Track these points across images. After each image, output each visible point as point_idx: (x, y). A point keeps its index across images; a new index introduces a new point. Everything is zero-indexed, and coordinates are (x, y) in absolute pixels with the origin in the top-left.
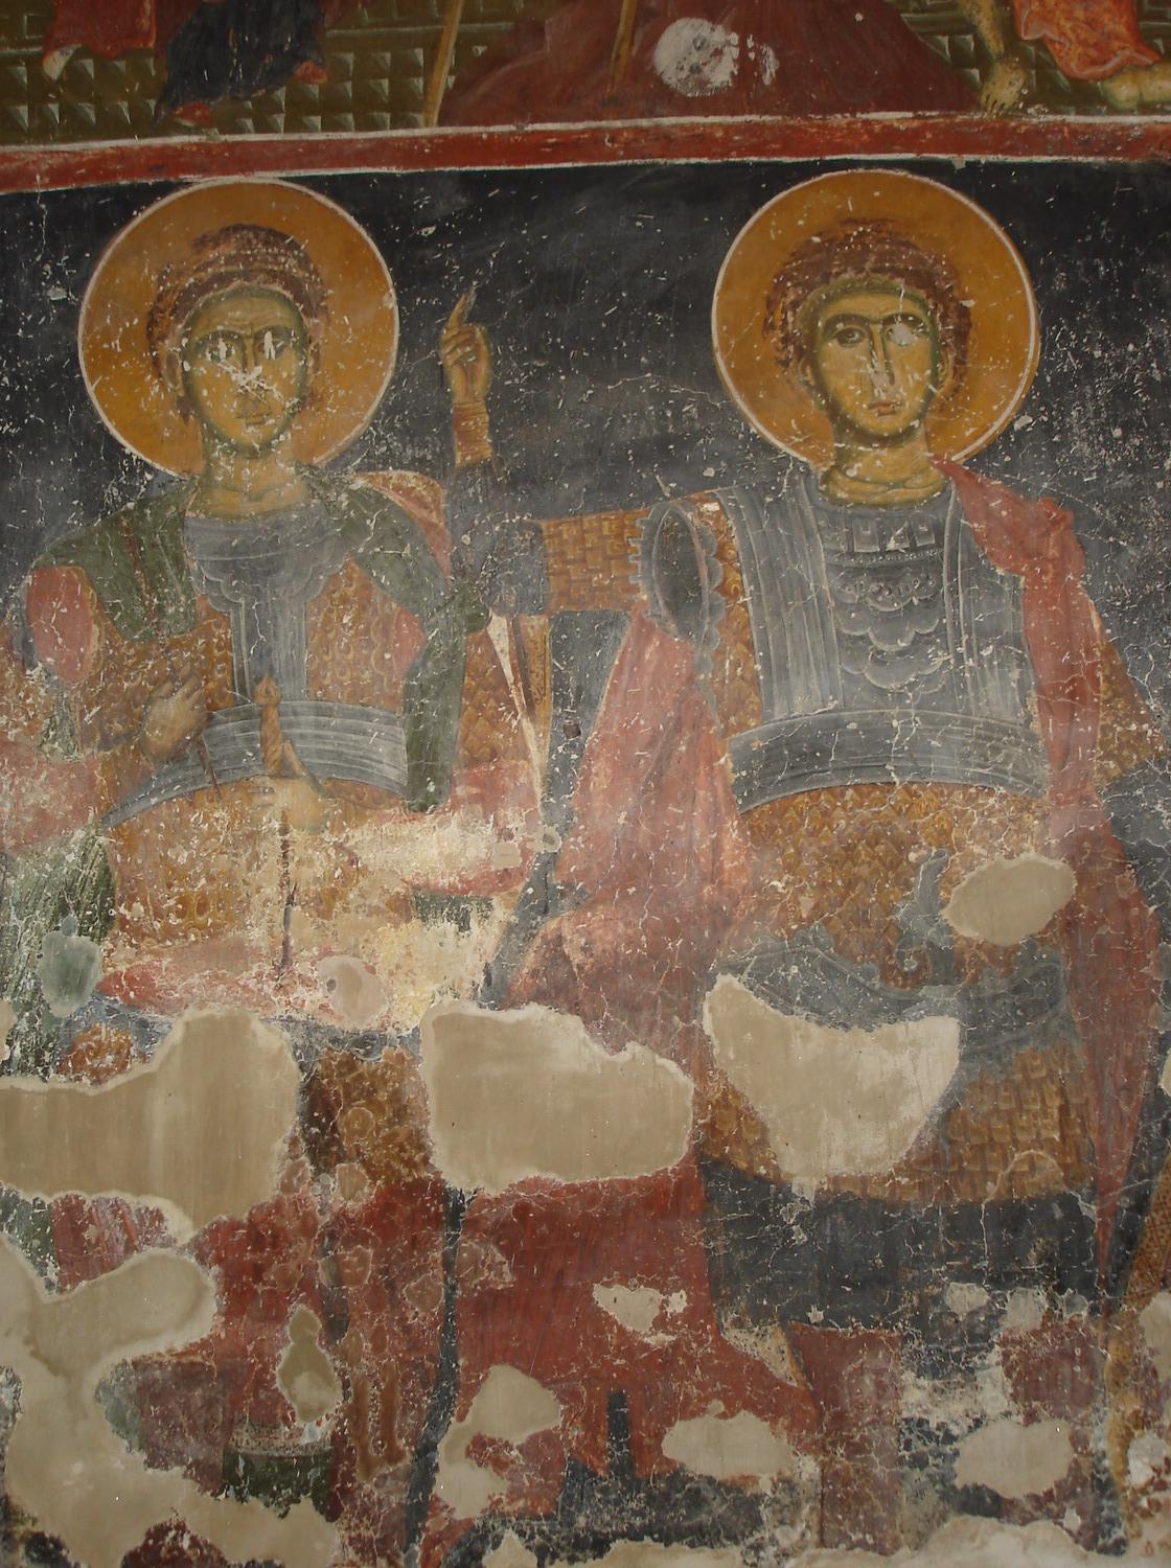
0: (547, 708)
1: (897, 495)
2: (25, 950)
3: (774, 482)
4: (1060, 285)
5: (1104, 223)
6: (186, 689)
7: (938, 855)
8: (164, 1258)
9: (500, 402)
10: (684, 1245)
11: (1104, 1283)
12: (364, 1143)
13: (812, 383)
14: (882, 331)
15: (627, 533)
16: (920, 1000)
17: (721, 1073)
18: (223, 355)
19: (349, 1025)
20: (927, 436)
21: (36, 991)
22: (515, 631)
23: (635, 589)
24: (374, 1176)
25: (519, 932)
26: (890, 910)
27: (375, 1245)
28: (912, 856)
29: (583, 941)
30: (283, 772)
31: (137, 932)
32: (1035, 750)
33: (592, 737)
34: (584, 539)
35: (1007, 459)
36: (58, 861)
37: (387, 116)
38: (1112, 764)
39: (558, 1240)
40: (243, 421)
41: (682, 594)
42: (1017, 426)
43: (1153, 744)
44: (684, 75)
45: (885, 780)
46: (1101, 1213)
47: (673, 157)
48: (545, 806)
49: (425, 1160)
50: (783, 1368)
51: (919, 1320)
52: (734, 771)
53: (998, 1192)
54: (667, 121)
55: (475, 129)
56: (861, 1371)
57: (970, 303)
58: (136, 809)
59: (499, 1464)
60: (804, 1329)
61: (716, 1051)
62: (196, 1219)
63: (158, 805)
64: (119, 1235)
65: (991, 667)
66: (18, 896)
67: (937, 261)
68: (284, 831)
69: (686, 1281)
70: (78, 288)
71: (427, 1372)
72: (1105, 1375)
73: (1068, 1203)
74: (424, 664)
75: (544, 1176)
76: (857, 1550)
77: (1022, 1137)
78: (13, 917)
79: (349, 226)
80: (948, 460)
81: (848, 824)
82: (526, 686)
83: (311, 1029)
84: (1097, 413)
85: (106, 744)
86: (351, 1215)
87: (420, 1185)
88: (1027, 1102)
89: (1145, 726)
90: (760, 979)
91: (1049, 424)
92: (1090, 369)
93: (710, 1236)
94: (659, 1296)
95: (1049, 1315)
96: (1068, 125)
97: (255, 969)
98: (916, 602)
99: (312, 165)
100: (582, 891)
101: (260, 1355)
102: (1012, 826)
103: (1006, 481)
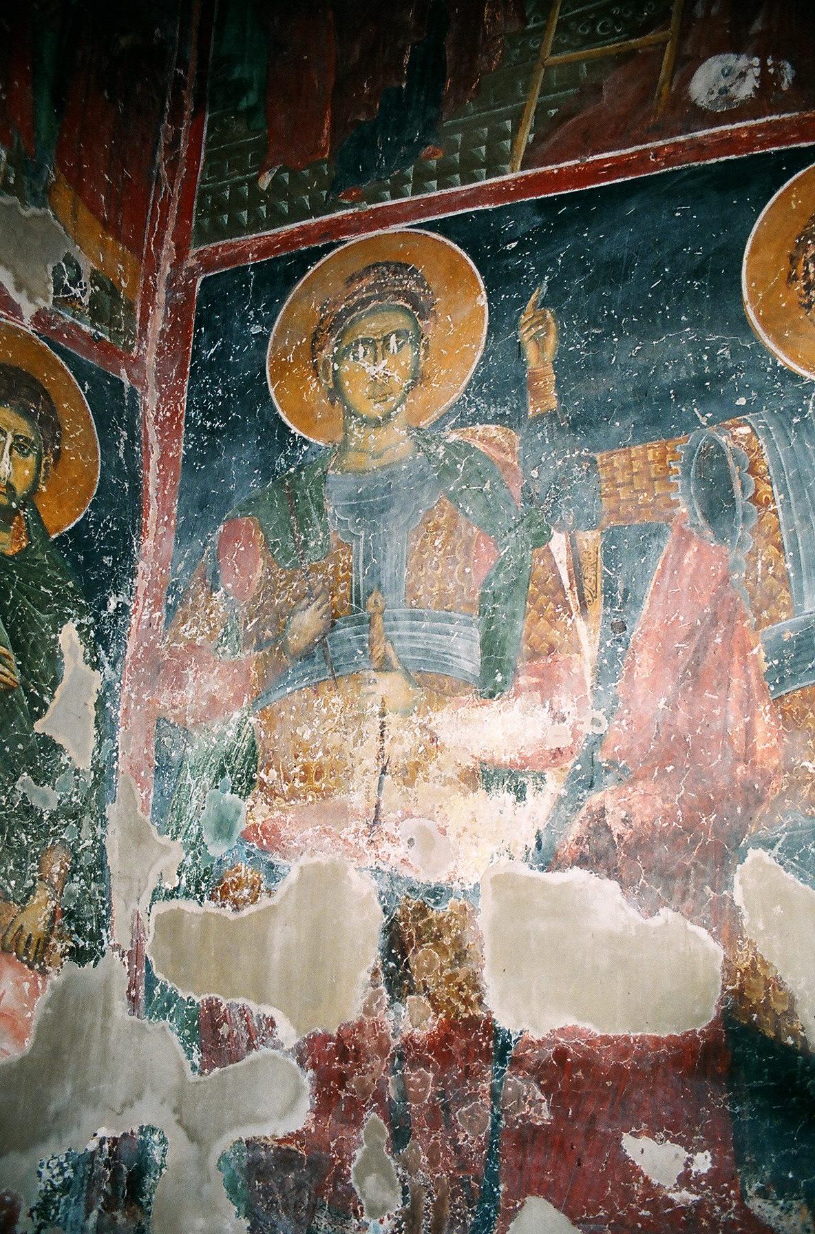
2: (195, 802)
3: (801, 405)
6: (318, 603)
8: (274, 1058)
9: (565, 366)
10: (710, 1107)
12: (430, 980)
15: (669, 457)
17: (750, 943)
18: (361, 355)
19: (424, 877)
21: (199, 835)
22: (572, 544)
24: (437, 1010)
25: (569, 803)
27: (434, 1070)
29: (624, 813)
30: (384, 666)
31: (272, 793)
33: (635, 633)
36: (221, 736)
37: (484, 170)
40: (372, 401)
41: (718, 504)
44: (713, 97)
47: (705, 160)
48: (595, 693)
49: (480, 1000)
52: (766, 660)
54: (700, 134)
55: (549, 168)
58: (275, 696)
61: (745, 922)
62: (298, 1028)
63: (292, 692)
64: (244, 1034)
68: (383, 714)
69: (711, 1143)
70: (269, 324)
71: (473, 1190)
74: (497, 575)
75: (581, 1026)
78: (189, 777)
79: (454, 251)
82: (580, 590)
83: (394, 879)
85: (259, 647)
86: (417, 1042)
87: (473, 1022)
90: (790, 855)
97: (353, 826)
99: (429, 215)
100: (625, 768)
101: (340, 1153)
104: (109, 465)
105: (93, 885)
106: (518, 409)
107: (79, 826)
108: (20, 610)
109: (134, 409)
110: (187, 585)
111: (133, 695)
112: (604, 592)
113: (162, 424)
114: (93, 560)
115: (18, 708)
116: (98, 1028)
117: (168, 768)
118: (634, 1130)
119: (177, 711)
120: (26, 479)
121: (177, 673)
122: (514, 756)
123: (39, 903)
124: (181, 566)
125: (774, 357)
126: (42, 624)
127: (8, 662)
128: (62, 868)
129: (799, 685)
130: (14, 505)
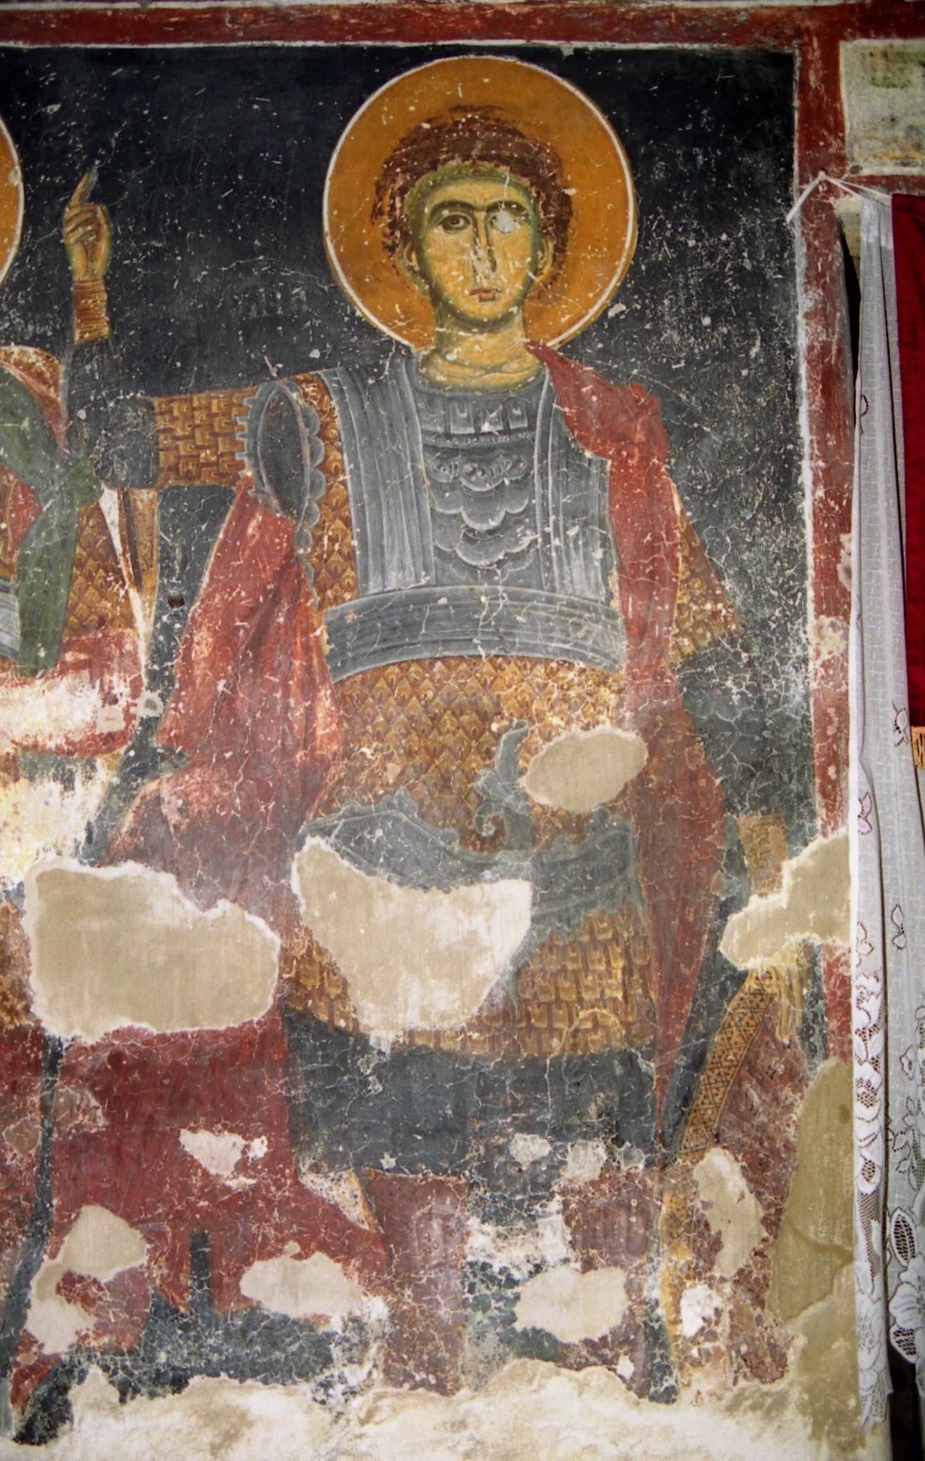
0: (153, 579)
1: (494, 379)
3: (377, 365)
4: (659, 175)
5: (705, 112)
7: (520, 726)
11: (661, 1137)
13: (417, 268)
14: (486, 218)
15: (234, 411)
16: (496, 864)
17: (307, 930)
20: (525, 321)
23: (241, 466)
25: (121, 792)
26: (471, 777)
28: (495, 727)
29: (180, 802)
32: (614, 627)
34: (193, 417)
35: (600, 346)
38: (686, 642)
39: (151, 1087)
42: (611, 314)
43: (726, 623)
45: (472, 652)
46: (659, 1069)
47: (289, 40)
49: (27, 1009)
50: (356, 1212)
51: (485, 1168)
53: (563, 1049)
56: (429, 1216)
57: (571, 192)
59: (87, 1301)
60: (377, 1175)
61: (302, 910)
65: (577, 548)
67: (541, 150)
69: (270, 1128)
71: (23, 1211)
72: (659, 1226)
73: (629, 1061)
75: (137, 1025)
76: (421, 1390)
77: (587, 996)
80: (544, 346)
81: (435, 695)
82: (134, 557)
84: (688, 302)
87: (20, 1033)
88: (593, 962)
89: (720, 606)
91: (642, 311)
92: (683, 258)
93: (291, 1085)
94: (240, 1141)
95: (606, 1167)
96: (676, 10)
98: (507, 482)
100: (181, 754)
102: (589, 699)
103: (596, 367)
106: (63, 330)
112: (161, 560)
118: (192, 1124)
122: (60, 741)
125: (353, 304)
129: (359, 669)
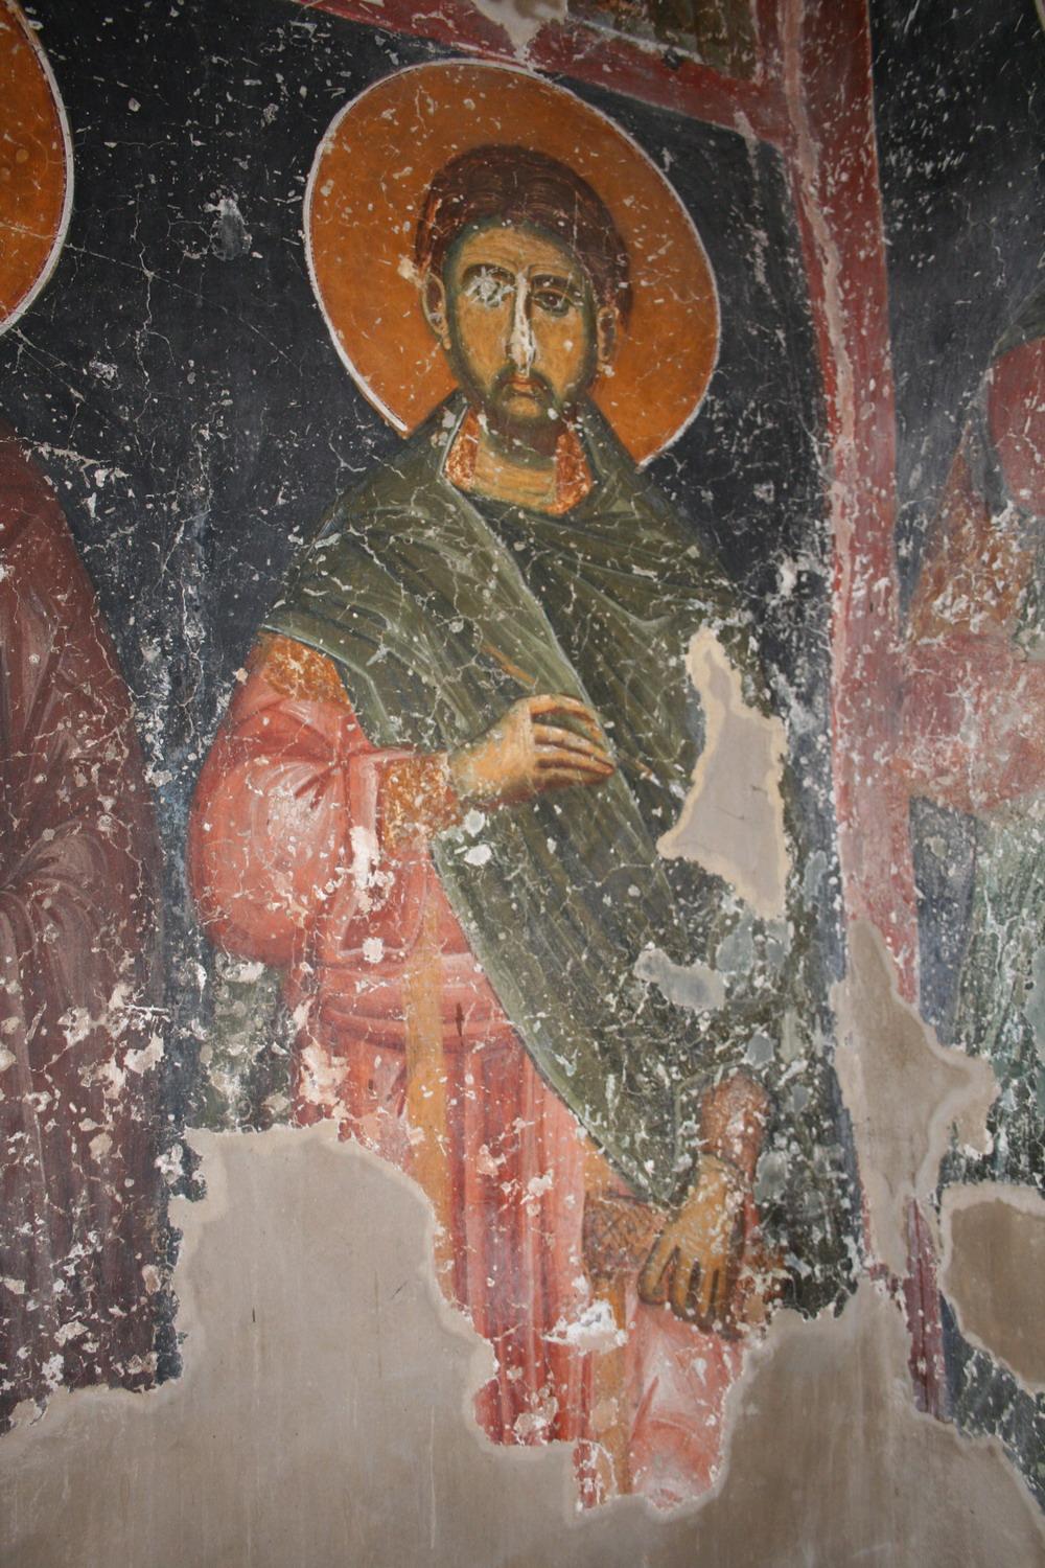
2: (1009, 973)
66: (995, 885)
104: (736, 303)
105: (818, 1152)
107: (776, 1034)
108: (595, 619)
109: (774, 184)
110: (933, 511)
111: (856, 757)
113: (834, 202)
114: (733, 495)
115: (619, 816)
116: (858, 1433)
117: (943, 903)
119: (947, 781)
120: (568, 359)
121: (939, 698)
123: (709, 1201)
124: (917, 474)
126: (646, 640)
127: (584, 726)
128: (748, 1123)
130: (552, 414)
